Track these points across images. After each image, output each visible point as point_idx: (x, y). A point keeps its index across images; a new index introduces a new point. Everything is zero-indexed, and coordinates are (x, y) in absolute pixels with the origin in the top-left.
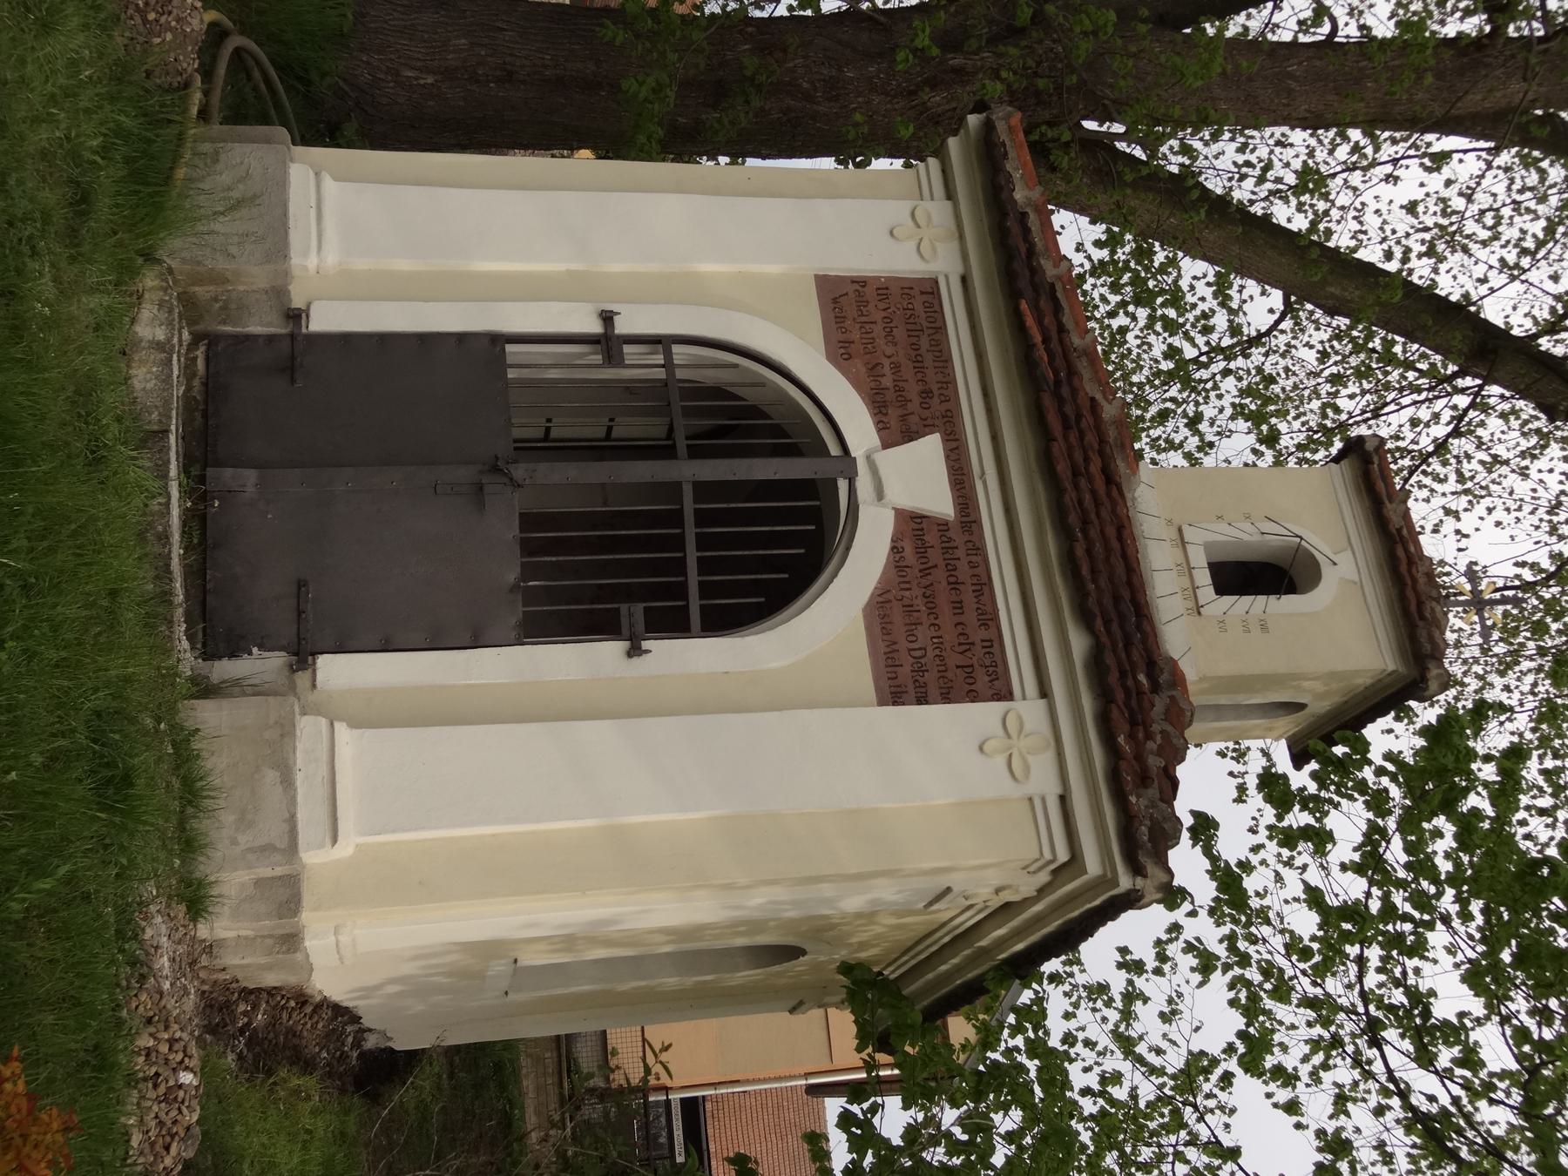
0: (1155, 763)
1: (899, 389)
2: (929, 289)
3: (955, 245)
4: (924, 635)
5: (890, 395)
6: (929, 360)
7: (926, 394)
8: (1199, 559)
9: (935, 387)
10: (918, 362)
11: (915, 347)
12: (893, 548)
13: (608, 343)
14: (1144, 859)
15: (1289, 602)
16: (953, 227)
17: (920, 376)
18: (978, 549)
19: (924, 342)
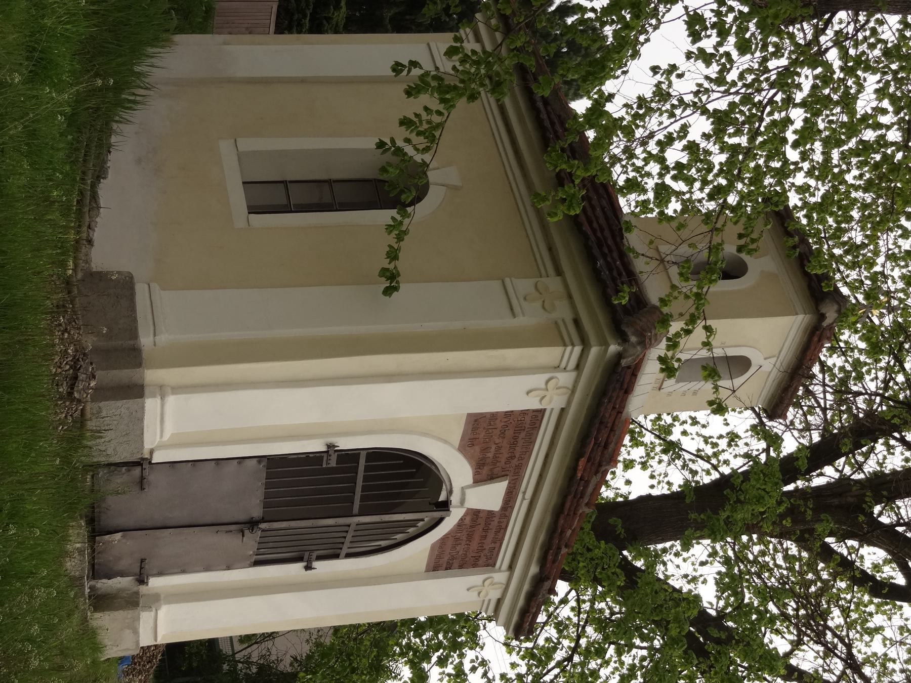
1: (495, 457)
10: (513, 444)
11: (515, 438)
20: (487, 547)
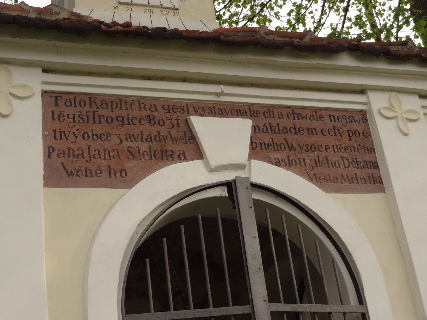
1: (149, 139)
2: (53, 100)
3: (14, 69)
4: (334, 157)
5: (156, 146)
6: (118, 112)
7: (150, 119)
9: (145, 113)
10: (122, 121)
11: (109, 120)
12: (276, 165)
17: (135, 121)
18: (269, 110)
20: (330, 125)
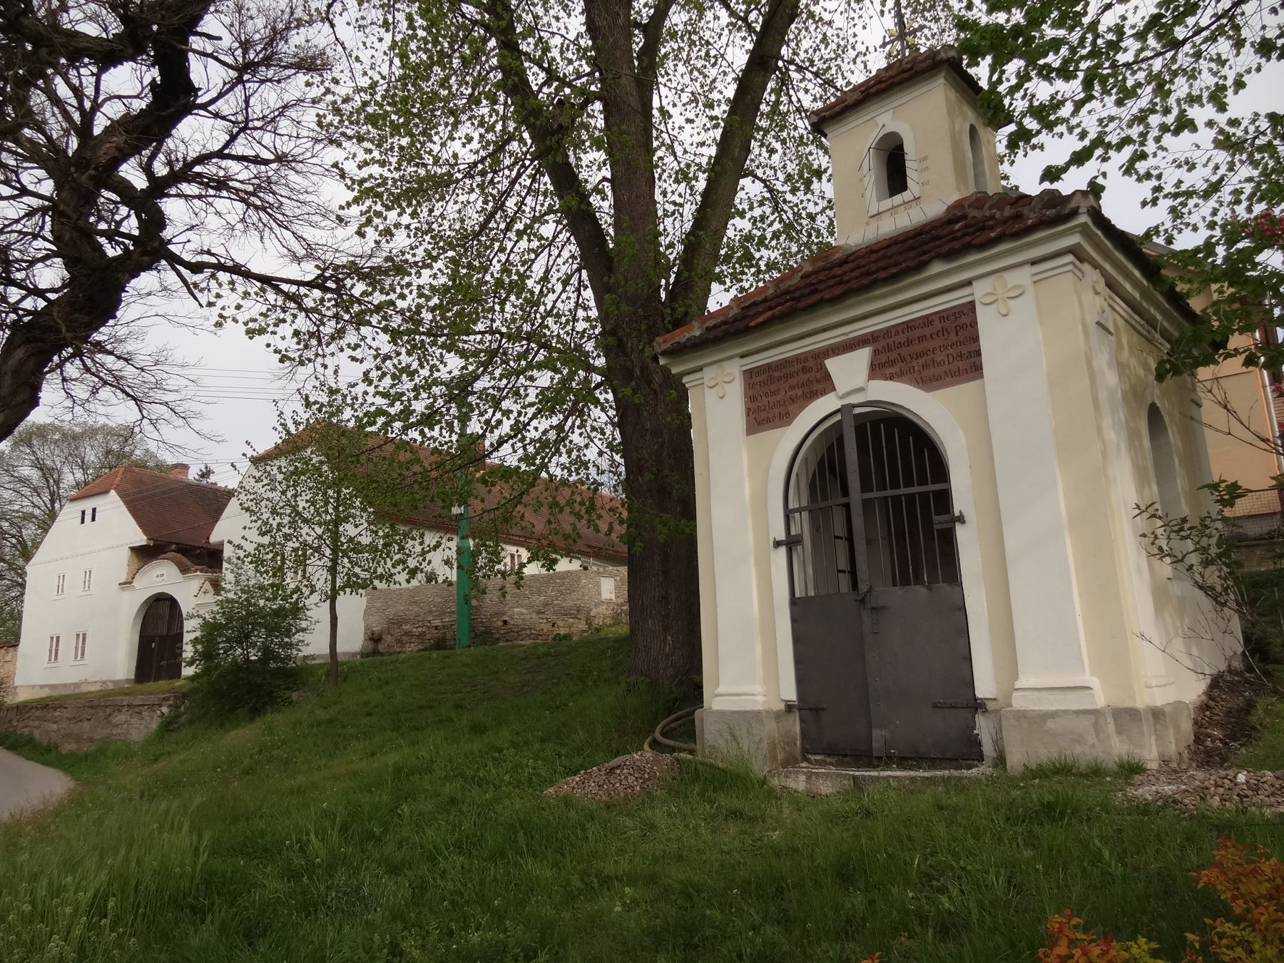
0: (1008, 211)
2: (749, 374)
3: (725, 363)
4: (940, 356)
5: (806, 390)
7: (804, 370)
8: (888, 203)
9: (800, 366)
10: (786, 376)
11: (779, 379)
13: (791, 543)
14: (1067, 210)
15: (907, 148)
16: (715, 367)
18: (888, 332)
19: (777, 374)
